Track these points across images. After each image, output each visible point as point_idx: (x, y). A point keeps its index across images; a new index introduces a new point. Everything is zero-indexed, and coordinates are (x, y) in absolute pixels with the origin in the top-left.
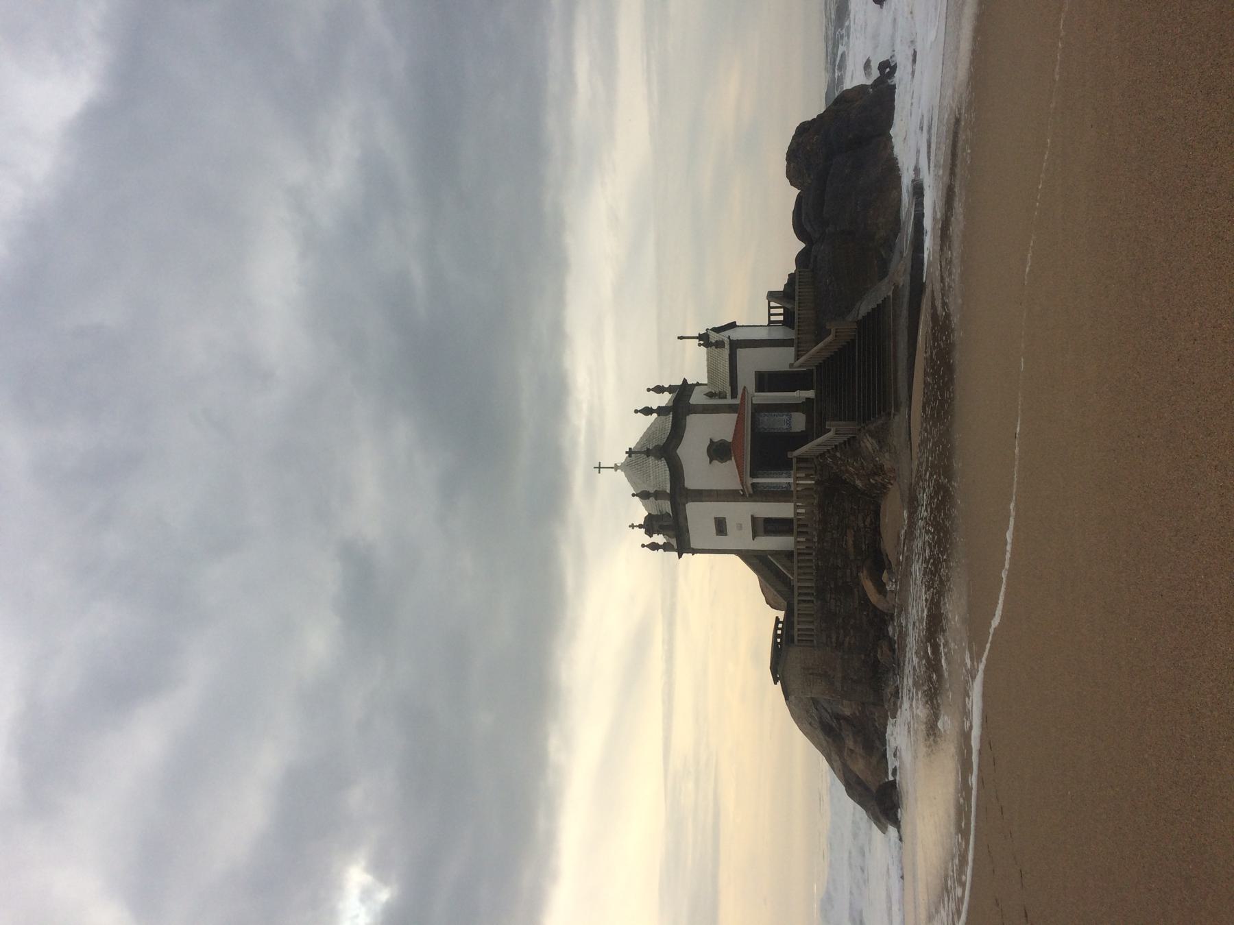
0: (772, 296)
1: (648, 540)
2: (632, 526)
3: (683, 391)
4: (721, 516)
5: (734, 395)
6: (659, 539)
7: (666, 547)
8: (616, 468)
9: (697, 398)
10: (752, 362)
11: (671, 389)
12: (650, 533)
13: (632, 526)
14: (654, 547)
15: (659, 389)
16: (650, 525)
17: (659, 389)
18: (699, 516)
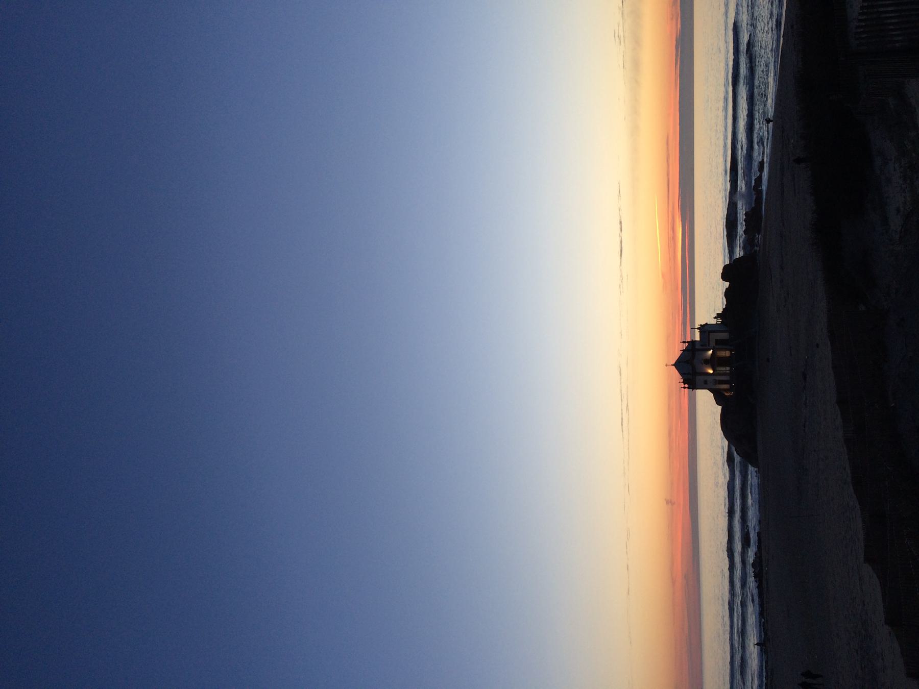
0: (717, 314)
1: (683, 386)
2: (680, 382)
3: (692, 343)
4: (705, 379)
5: (709, 345)
6: (686, 386)
7: (688, 388)
8: (672, 365)
9: (697, 347)
10: (714, 337)
11: (688, 342)
12: (685, 384)
13: (680, 382)
14: (684, 388)
15: (684, 342)
16: (684, 383)
17: (684, 342)
18: (699, 379)
